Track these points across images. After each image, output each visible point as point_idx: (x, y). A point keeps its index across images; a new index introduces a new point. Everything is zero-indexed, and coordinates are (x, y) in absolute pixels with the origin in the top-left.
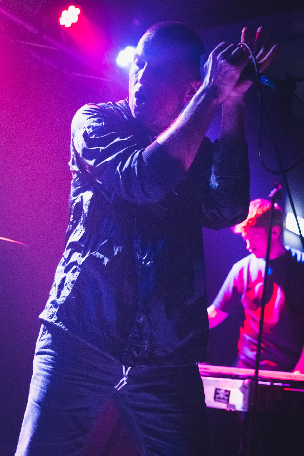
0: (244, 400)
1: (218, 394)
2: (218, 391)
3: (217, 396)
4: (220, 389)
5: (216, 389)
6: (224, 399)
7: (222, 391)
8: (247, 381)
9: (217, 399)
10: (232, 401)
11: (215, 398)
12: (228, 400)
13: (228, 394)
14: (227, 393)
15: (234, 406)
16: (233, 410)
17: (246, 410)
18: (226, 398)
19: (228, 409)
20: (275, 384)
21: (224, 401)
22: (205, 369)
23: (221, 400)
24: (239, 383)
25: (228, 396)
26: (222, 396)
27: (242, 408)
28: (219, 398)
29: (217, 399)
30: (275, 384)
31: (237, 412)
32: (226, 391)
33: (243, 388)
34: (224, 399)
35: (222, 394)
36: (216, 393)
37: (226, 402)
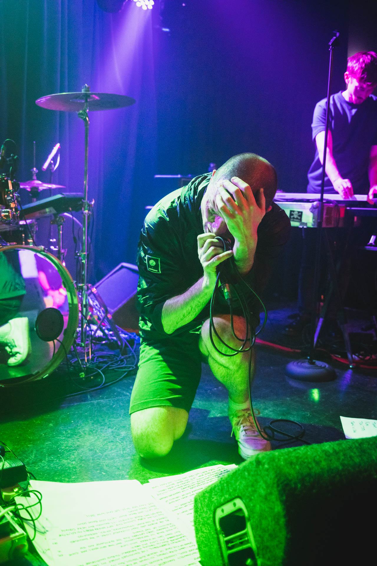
0: (314, 218)
1: (293, 215)
2: (292, 213)
4: (294, 211)
5: (291, 211)
7: (296, 213)
8: (315, 203)
10: (304, 220)
12: (301, 220)
13: (300, 214)
14: (300, 214)
15: (306, 224)
16: (305, 227)
17: (316, 226)
18: (299, 218)
19: (301, 227)
21: (298, 220)
23: (295, 220)
24: (309, 205)
26: (295, 216)
27: (313, 225)
28: (294, 218)
30: (340, 205)
31: (308, 228)
32: (299, 212)
33: (313, 210)
34: (297, 218)
37: (299, 221)
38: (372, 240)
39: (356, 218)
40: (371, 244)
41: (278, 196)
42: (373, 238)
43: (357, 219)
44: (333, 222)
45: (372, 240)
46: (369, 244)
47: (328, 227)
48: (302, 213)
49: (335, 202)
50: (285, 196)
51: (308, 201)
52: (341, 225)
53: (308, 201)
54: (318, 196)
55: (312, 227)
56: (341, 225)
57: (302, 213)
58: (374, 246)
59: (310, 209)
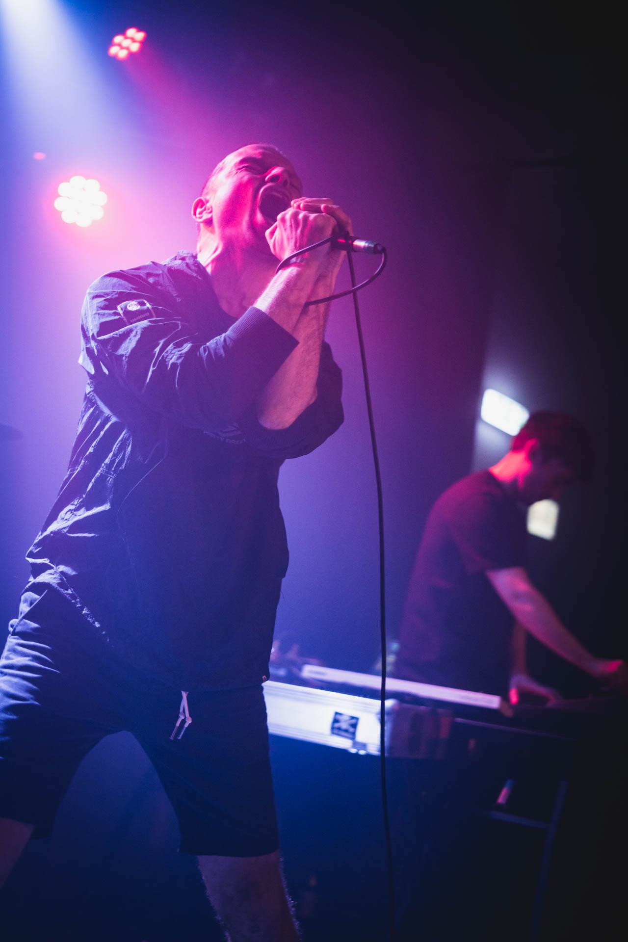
2: (338, 717)
3: (337, 725)
4: (341, 714)
10: (360, 737)
11: (333, 728)
12: (354, 734)
13: (354, 723)
14: (354, 721)
15: (364, 746)
16: (362, 752)
18: (351, 730)
19: (353, 751)
25: (354, 726)
26: (344, 725)
28: (339, 729)
29: (336, 731)
31: (368, 756)
32: (353, 718)
34: (346, 731)
36: (336, 721)
37: (351, 736)
38: (502, 798)
41: (311, 672)
45: (502, 798)
50: (323, 674)
57: (357, 719)
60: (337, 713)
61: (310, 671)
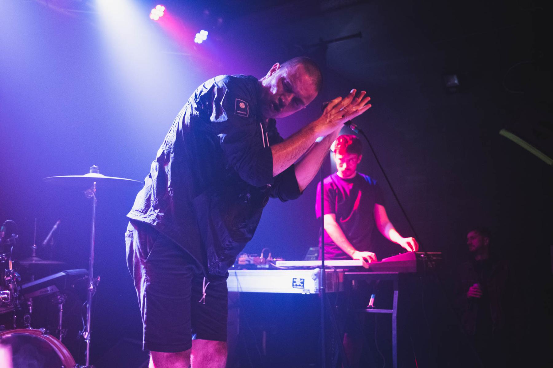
1: (295, 282)
2: (295, 280)
3: (295, 284)
4: (296, 279)
5: (293, 279)
6: (300, 285)
9: (295, 286)
11: (293, 285)
12: (303, 286)
14: (302, 281)
15: (309, 290)
16: (308, 293)
17: (318, 293)
18: (302, 285)
20: (338, 270)
22: (283, 264)
23: (297, 287)
25: (303, 283)
26: (298, 283)
27: (315, 292)
28: (296, 285)
29: (295, 286)
30: (338, 270)
32: (301, 279)
34: (300, 285)
35: (298, 281)
36: (294, 282)
37: (302, 287)
38: (371, 303)
39: (353, 282)
40: (370, 306)
41: (279, 264)
42: (372, 300)
43: (355, 283)
44: (333, 287)
45: (371, 303)
46: (368, 306)
47: (329, 292)
48: (304, 280)
49: (334, 268)
50: (285, 264)
51: (308, 268)
52: (341, 289)
53: (308, 268)
54: (319, 263)
55: (314, 293)
56: (341, 289)
57: (304, 280)
58: (374, 308)
59: (311, 276)
60: (293, 279)
61: (280, 263)
